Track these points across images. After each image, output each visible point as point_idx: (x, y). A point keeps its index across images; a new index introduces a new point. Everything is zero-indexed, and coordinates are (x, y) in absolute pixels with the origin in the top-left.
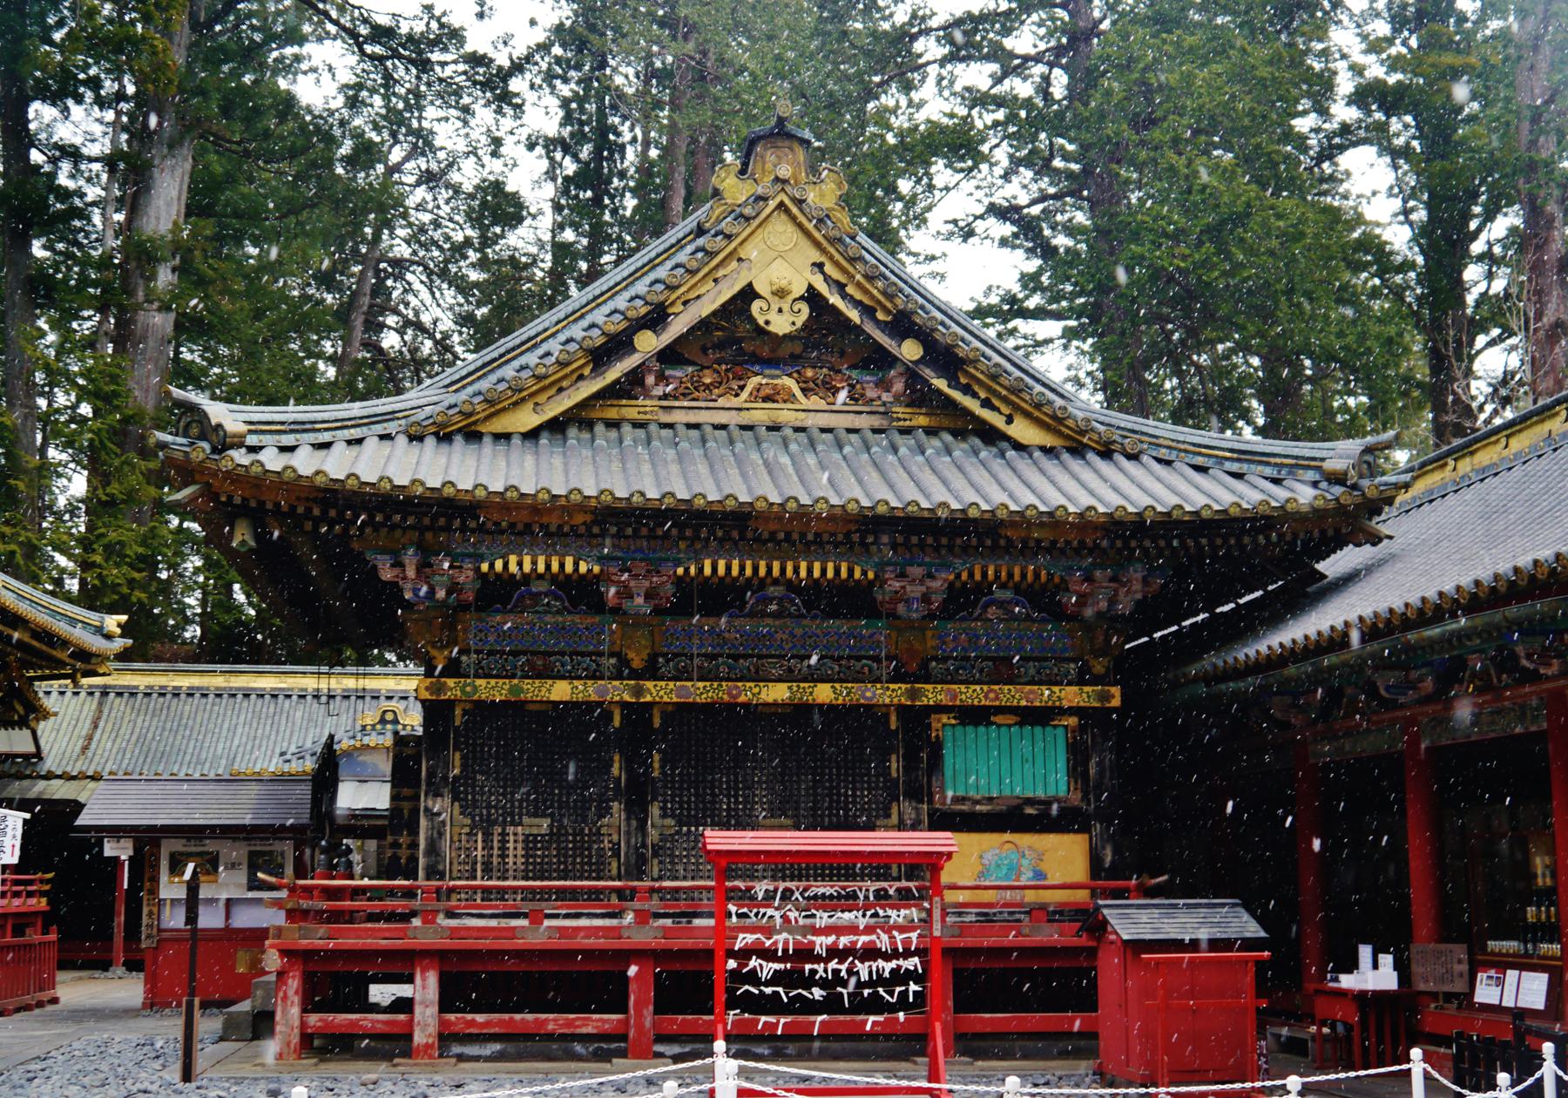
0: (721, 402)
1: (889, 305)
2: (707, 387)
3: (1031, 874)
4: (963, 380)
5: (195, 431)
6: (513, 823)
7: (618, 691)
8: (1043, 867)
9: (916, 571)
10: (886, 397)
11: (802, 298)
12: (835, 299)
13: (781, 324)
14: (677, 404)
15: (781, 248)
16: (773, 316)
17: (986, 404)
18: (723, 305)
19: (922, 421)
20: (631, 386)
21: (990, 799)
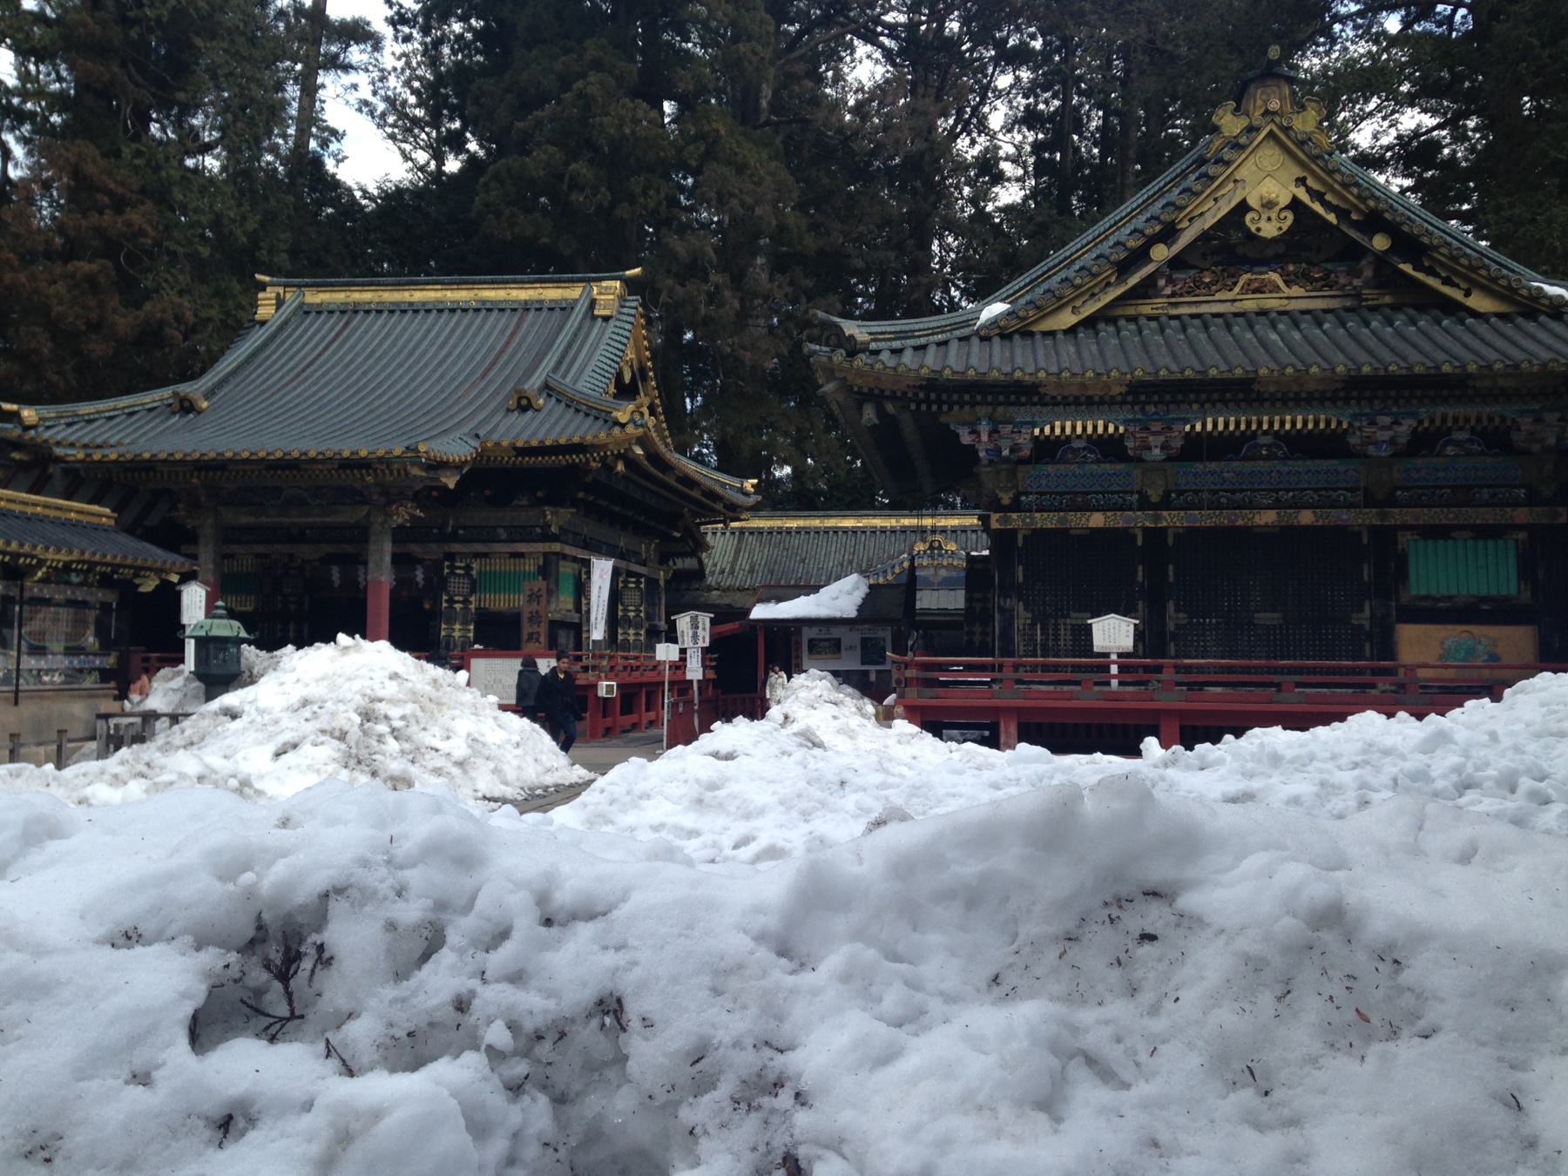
0: (1218, 296)
1: (1362, 207)
2: (1207, 286)
3: (1486, 657)
4: (1426, 264)
5: (833, 340)
6: (1062, 617)
7: (1140, 520)
9: (1386, 420)
10: (1356, 282)
11: (1287, 208)
12: (1317, 207)
13: (1269, 230)
14: (1181, 299)
15: (1270, 168)
16: (1263, 224)
17: (1447, 281)
18: (1219, 221)
19: (1388, 299)
20: (1146, 289)
21: (1450, 598)
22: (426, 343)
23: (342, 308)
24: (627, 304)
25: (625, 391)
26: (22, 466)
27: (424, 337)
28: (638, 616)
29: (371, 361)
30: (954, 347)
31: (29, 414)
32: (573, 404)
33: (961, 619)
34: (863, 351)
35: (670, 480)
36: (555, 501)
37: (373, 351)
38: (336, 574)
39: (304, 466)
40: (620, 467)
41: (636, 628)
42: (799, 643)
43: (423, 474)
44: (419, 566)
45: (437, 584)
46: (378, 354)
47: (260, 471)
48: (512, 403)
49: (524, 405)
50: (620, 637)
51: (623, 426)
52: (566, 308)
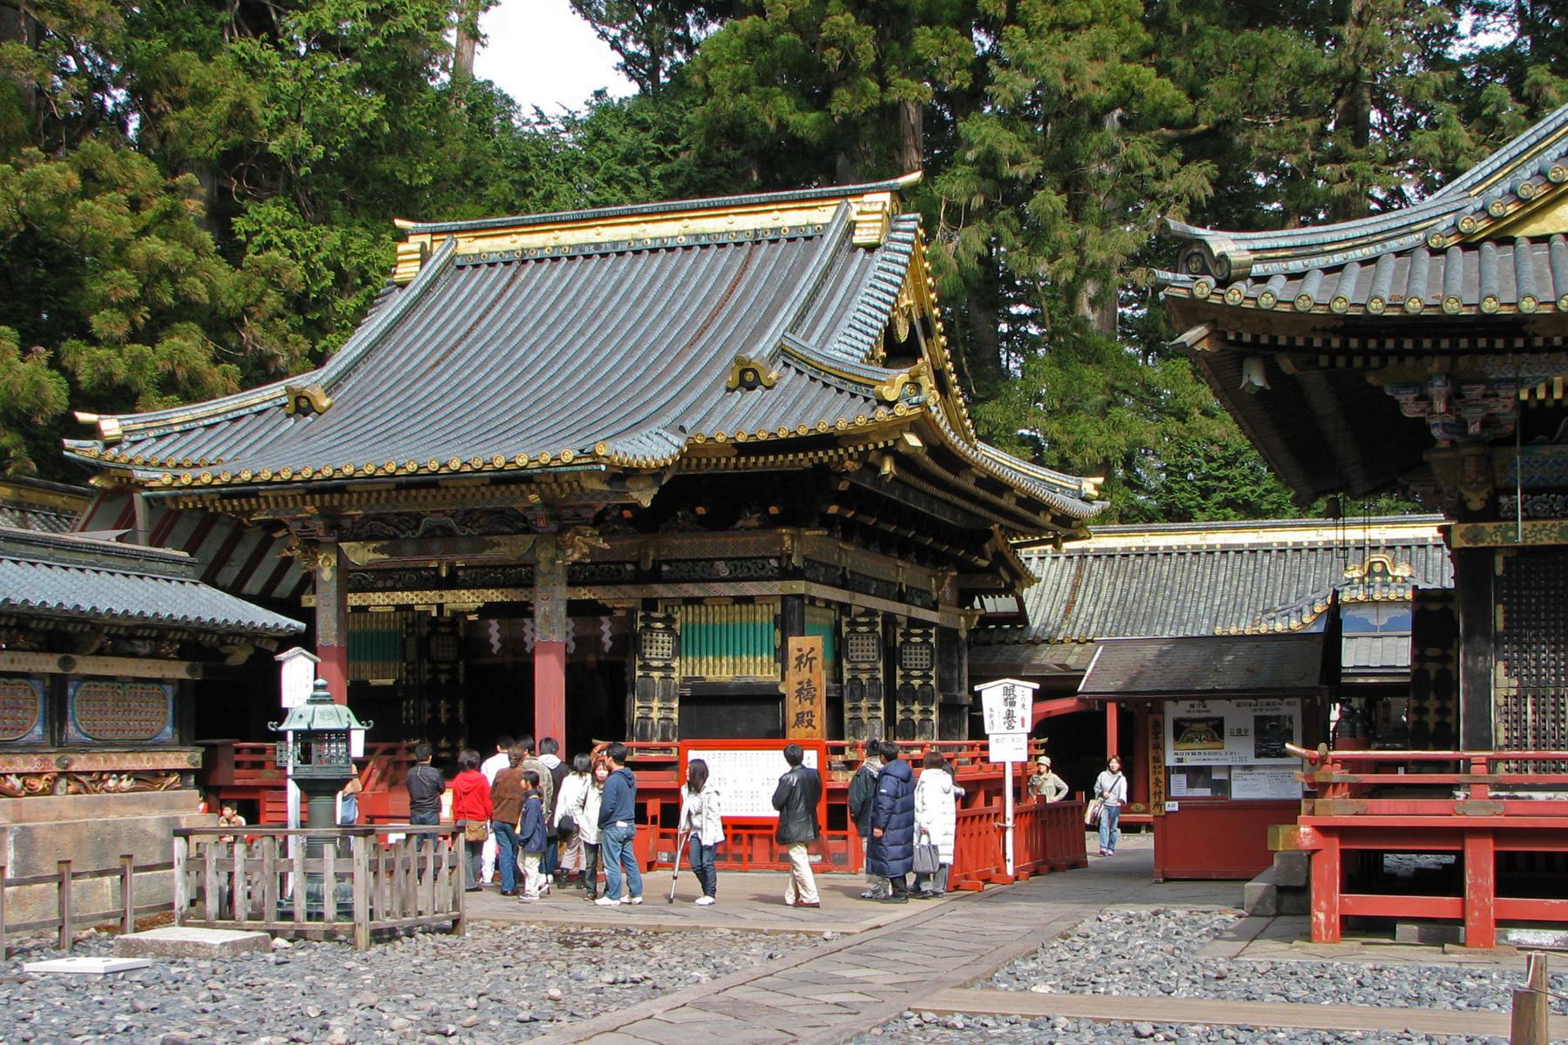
22: (617, 299)
23: (507, 258)
24: (901, 226)
25: (898, 352)
26: (104, 494)
27: (614, 291)
28: (926, 684)
29: (543, 329)
30: (1389, 265)
31: (111, 425)
33: (1408, 680)
34: (1243, 278)
35: (968, 484)
36: (793, 518)
37: (545, 316)
38: (494, 628)
39: (450, 483)
40: (888, 467)
41: (923, 702)
42: (1159, 727)
43: (605, 488)
44: (604, 619)
45: (629, 643)
46: (551, 320)
47: (388, 491)
48: (732, 379)
49: (747, 379)
50: (899, 717)
51: (891, 405)
52: (811, 237)
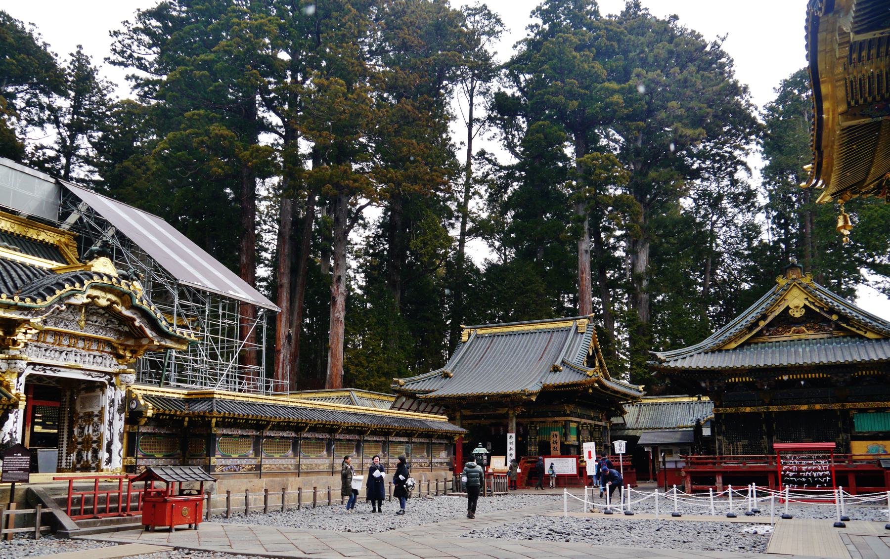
0: (785, 335)
8: (886, 449)
9: (841, 375)
10: (831, 329)
12: (812, 307)
13: (797, 315)
16: (795, 313)
17: (858, 329)
21: (869, 432)
32: (572, 368)
